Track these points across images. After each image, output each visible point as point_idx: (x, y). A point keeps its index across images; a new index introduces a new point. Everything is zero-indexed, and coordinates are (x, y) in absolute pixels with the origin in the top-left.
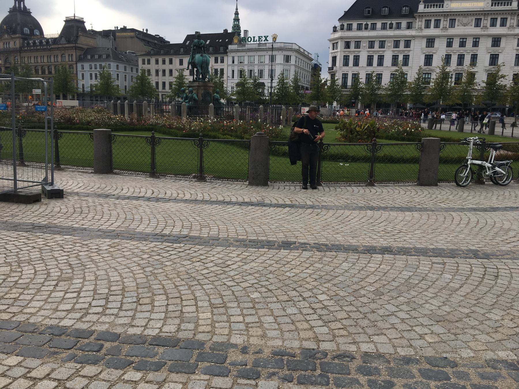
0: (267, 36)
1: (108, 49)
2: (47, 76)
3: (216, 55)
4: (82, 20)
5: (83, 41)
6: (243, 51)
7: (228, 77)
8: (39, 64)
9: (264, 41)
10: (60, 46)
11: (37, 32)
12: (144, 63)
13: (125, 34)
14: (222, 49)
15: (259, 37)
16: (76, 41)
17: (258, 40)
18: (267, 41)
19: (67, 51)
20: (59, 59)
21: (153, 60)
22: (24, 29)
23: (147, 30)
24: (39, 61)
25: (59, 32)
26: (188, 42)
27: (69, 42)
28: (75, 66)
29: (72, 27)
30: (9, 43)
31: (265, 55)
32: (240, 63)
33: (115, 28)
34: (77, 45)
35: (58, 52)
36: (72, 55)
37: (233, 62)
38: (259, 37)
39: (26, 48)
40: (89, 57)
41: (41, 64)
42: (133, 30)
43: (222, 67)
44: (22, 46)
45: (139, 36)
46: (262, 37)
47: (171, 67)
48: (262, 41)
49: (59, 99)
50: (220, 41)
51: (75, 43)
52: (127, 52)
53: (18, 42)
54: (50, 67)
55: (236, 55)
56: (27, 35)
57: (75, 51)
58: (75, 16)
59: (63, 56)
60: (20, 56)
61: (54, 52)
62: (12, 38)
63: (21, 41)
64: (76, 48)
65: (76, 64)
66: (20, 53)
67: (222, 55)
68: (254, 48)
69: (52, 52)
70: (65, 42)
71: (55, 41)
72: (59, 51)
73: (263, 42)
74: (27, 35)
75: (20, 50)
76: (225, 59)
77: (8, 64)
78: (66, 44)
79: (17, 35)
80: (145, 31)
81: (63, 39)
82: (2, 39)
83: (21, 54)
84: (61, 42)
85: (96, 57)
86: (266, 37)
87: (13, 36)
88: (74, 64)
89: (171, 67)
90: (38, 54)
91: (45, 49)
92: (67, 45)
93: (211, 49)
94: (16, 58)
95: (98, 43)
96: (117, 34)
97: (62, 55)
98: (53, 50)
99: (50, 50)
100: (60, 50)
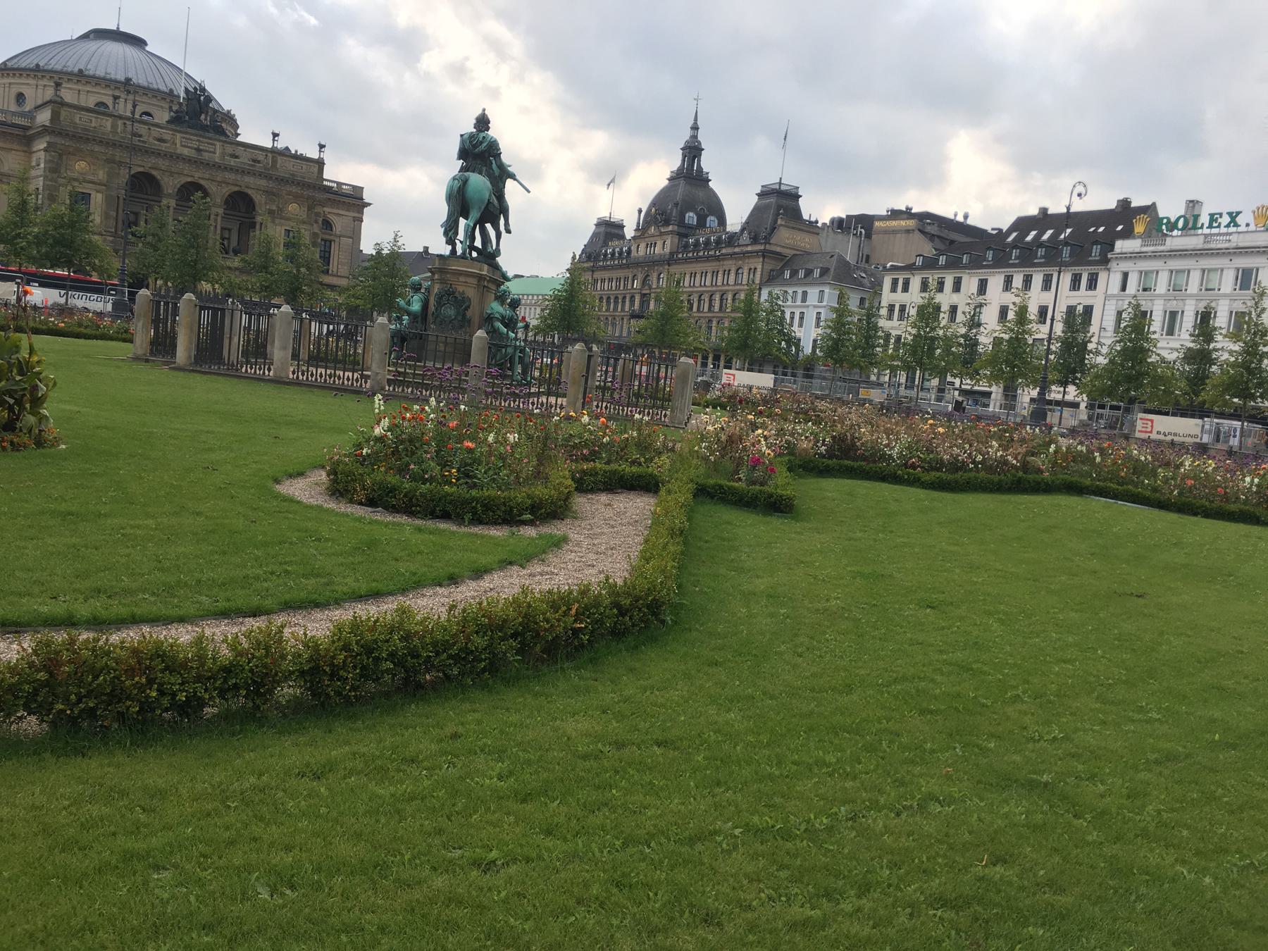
0: (1238, 213)
1: (832, 256)
2: (706, 315)
3: (1077, 269)
4: (794, 191)
5: (786, 238)
6: (1155, 256)
7: (1102, 329)
8: (695, 289)
9: (1228, 226)
10: (737, 250)
11: (712, 221)
12: (894, 290)
13: (894, 223)
14: (1096, 250)
15: (1212, 215)
16: (767, 240)
17: (1206, 225)
18: (1236, 225)
19: (747, 261)
21: (915, 283)
22: (687, 215)
23: (966, 217)
24: (697, 284)
25: (744, 221)
26: (1014, 234)
27: (755, 240)
29: (767, 207)
30: (656, 243)
31: (1222, 270)
32: (1145, 290)
33: (888, 211)
34: (768, 247)
35: (730, 262)
36: (755, 269)
37: (1124, 288)
38: (1212, 215)
39: (680, 256)
40: (787, 274)
41: (699, 289)
42: (925, 217)
43: (1088, 302)
44: (675, 250)
45: (929, 229)
46: (1221, 215)
47: (955, 299)
48: (1219, 226)
49: (730, 368)
50: (1101, 229)
51: (765, 243)
52: (888, 265)
53: (668, 242)
54: (725, 297)
55: (1133, 268)
56: (690, 227)
57: (761, 259)
58: (780, 183)
59: (740, 271)
61: (725, 263)
62: (662, 234)
63: (676, 240)
64: (765, 254)
65: (760, 289)
67: (1093, 269)
68: (1191, 247)
69: (721, 263)
70: (748, 242)
71: (733, 239)
72: (734, 262)
73: (1223, 230)
74: (689, 228)
75: (670, 260)
76: (1102, 277)
78: (747, 245)
79: (670, 228)
80: (960, 218)
81: (746, 234)
82: (646, 235)
84: (741, 242)
85: (801, 274)
86: (1233, 216)
89: (955, 299)
90: (698, 267)
91: (712, 256)
93: (1066, 252)
94: (662, 276)
95: (823, 244)
96: (877, 224)
97: (738, 270)
98: (723, 260)
99: (717, 258)
100: (736, 258)
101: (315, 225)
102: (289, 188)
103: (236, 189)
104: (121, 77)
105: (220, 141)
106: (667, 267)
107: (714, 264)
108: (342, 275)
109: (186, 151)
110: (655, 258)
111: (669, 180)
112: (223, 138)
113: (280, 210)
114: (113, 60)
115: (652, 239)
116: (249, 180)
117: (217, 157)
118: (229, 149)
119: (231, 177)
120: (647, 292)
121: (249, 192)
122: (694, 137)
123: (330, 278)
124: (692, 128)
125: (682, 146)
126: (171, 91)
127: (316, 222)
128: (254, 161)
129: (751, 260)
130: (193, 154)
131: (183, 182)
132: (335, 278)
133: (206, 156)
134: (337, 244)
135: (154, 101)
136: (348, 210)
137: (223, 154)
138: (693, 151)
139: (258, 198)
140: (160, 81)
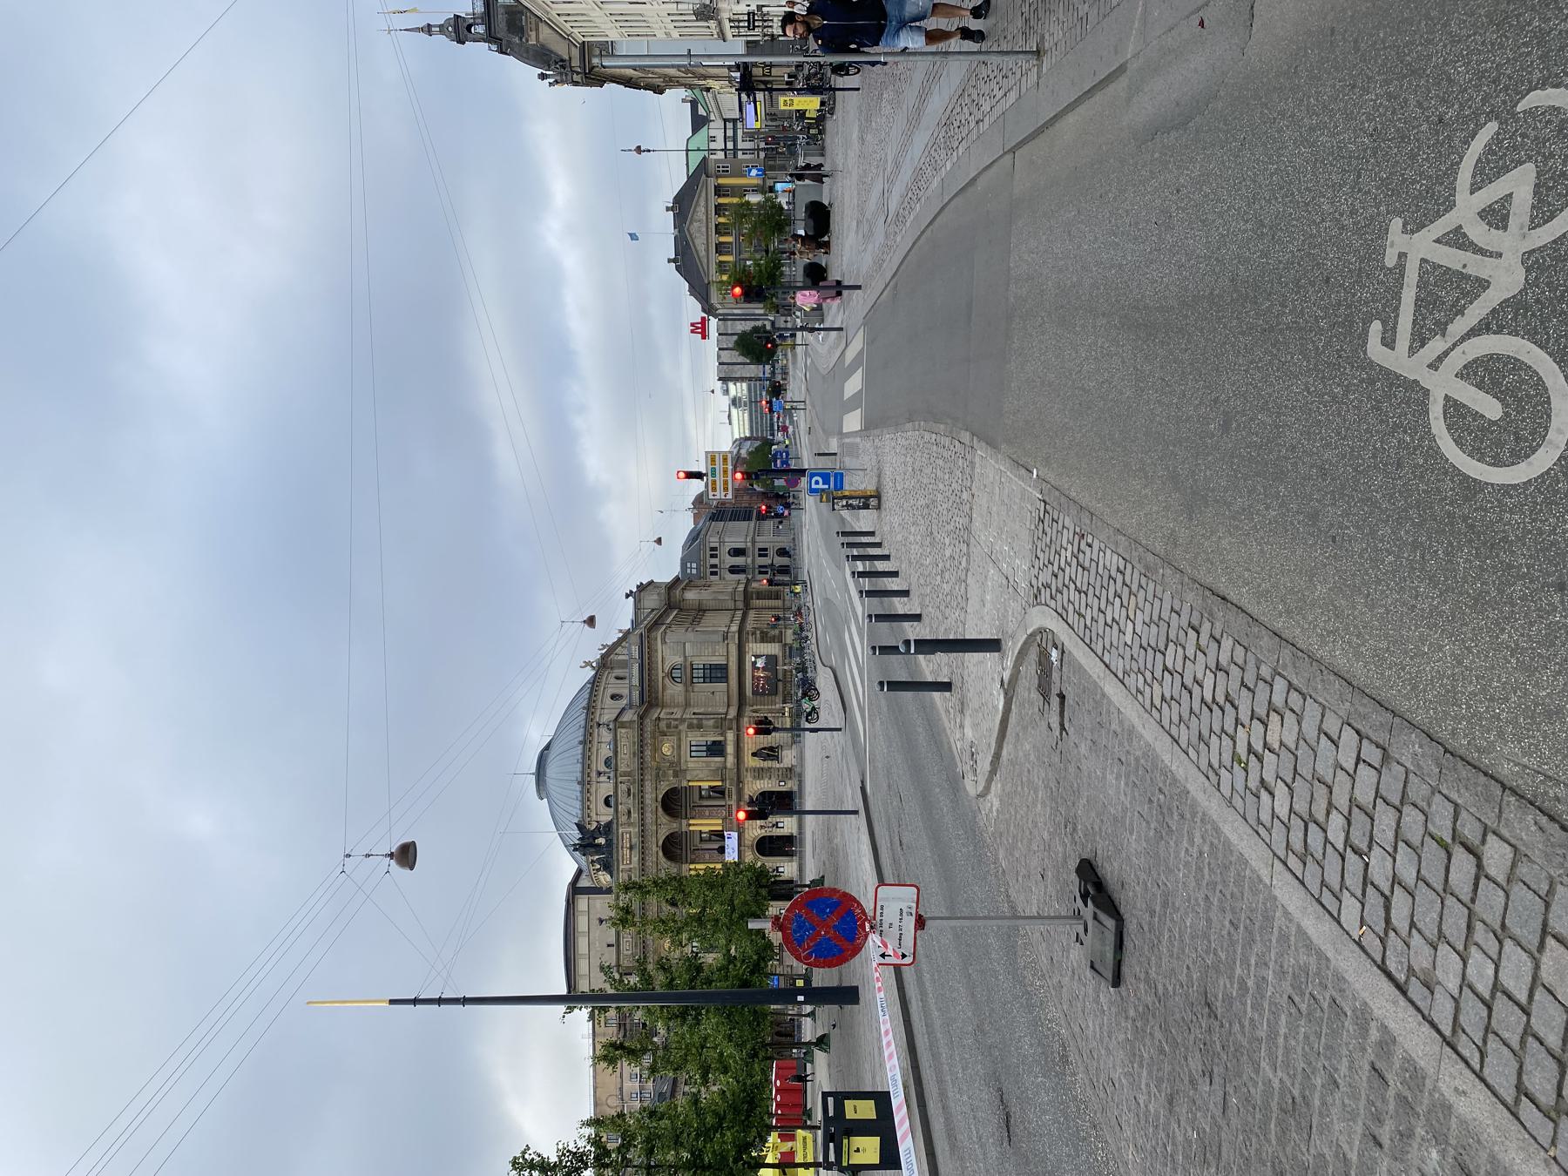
101: (681, 727)
102: (648, 759)
103: (660, 809)
104: (578, 788)
105: (617, 829)
108: (725, 649)
109: (635, 859)
112: (615, 826)
113: (672, 763)
114: (564, 769)
116: (649, 798)
117: (635, 830)
118: (623, 819)
119: (649, 817)
121: (660, 797)
122: (442, 29)
123: (730, 664)
126: (580, 743)
127: (676, 727)
128: (629, 795)
130: (636, 853)
131: (664, 860)
132: (731, 659)
133: (634, 840)
134: (693, 659)
135: (594, 758)
136: (656, 651)
137: (630, 824)
138: (459, 30)
139: (664, 787)
140: (573, 752)
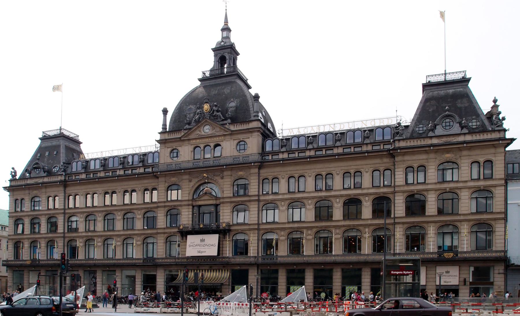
19: (465, 153)
20: (432, 175)
28: (499, 192)
44: (261, 152)
60: (259, 176)
61: (407, 158)
65: (506, 183)
66: (260, 168)
77: (206, 197)
82: (191, 137)
83: (262, 171)
84: (439, 131)
87: (232, 128)
88: (495, 186)
92: (468, 138)
98: (404, 154)
106: (256, 170)
107: (378, 161)
110: (222, 162)
111: (200, 80)
115: (207, 140)
120: (214, 202)
124: (223, 30)
125: (214, 47)
129: (478, 152)
